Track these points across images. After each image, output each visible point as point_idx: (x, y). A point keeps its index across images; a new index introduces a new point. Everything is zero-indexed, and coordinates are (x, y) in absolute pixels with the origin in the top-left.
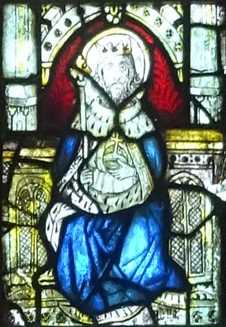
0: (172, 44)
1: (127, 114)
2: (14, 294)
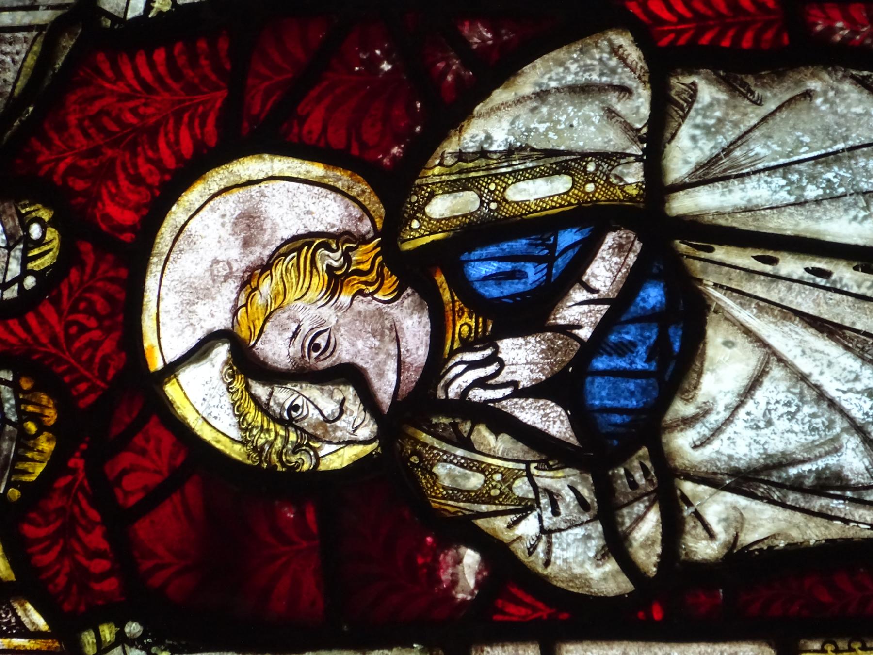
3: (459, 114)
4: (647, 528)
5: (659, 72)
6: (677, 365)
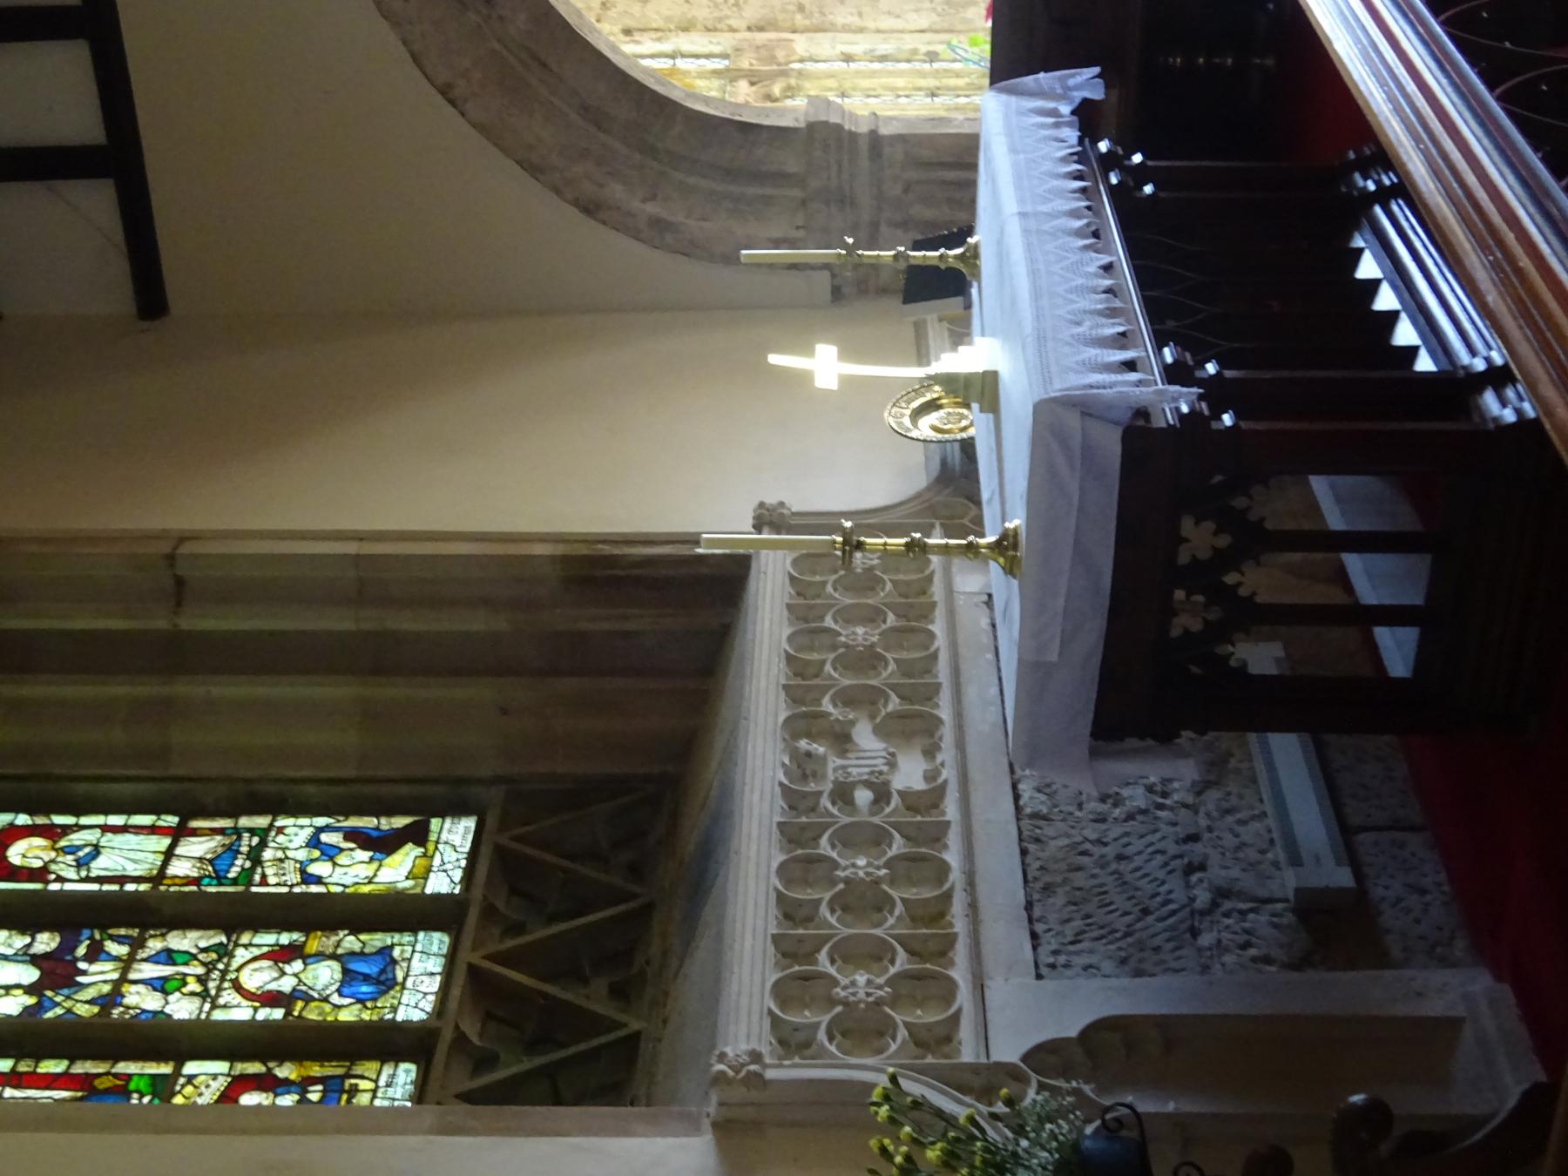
0: (256, 952)
2: (375, 1018)
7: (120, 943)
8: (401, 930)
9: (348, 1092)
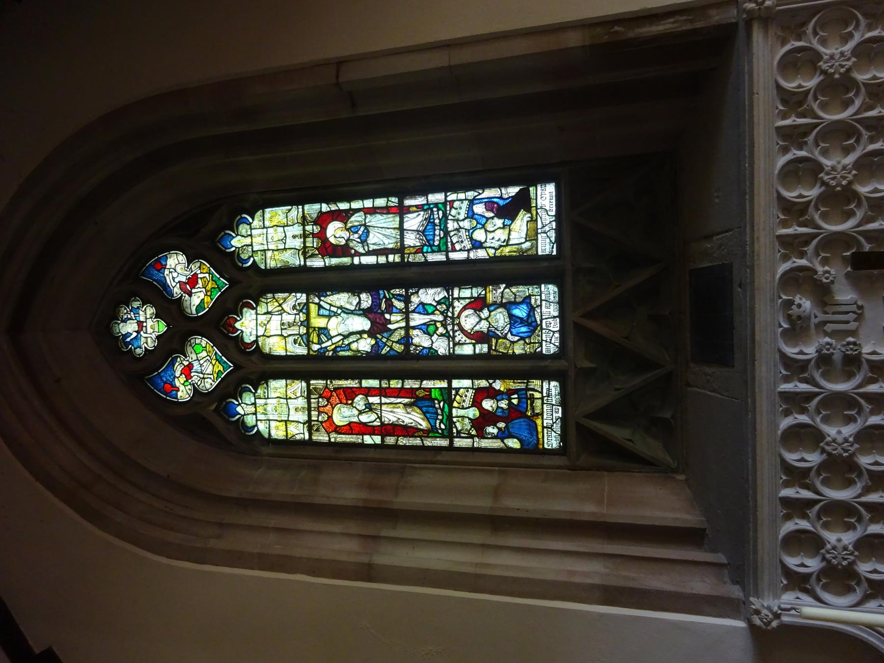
0: (464, 302)
1: (483, 317)
2: (532, 351)
3: (349, 218)
4: (366, 248)
5: (365, 214)
6: (368, 236)
7: (399, 300)
8: (532, 284)
9: (530, 399)
